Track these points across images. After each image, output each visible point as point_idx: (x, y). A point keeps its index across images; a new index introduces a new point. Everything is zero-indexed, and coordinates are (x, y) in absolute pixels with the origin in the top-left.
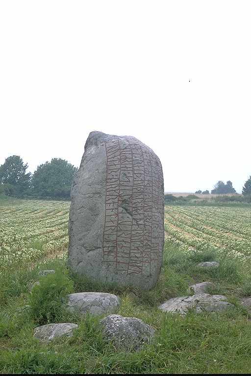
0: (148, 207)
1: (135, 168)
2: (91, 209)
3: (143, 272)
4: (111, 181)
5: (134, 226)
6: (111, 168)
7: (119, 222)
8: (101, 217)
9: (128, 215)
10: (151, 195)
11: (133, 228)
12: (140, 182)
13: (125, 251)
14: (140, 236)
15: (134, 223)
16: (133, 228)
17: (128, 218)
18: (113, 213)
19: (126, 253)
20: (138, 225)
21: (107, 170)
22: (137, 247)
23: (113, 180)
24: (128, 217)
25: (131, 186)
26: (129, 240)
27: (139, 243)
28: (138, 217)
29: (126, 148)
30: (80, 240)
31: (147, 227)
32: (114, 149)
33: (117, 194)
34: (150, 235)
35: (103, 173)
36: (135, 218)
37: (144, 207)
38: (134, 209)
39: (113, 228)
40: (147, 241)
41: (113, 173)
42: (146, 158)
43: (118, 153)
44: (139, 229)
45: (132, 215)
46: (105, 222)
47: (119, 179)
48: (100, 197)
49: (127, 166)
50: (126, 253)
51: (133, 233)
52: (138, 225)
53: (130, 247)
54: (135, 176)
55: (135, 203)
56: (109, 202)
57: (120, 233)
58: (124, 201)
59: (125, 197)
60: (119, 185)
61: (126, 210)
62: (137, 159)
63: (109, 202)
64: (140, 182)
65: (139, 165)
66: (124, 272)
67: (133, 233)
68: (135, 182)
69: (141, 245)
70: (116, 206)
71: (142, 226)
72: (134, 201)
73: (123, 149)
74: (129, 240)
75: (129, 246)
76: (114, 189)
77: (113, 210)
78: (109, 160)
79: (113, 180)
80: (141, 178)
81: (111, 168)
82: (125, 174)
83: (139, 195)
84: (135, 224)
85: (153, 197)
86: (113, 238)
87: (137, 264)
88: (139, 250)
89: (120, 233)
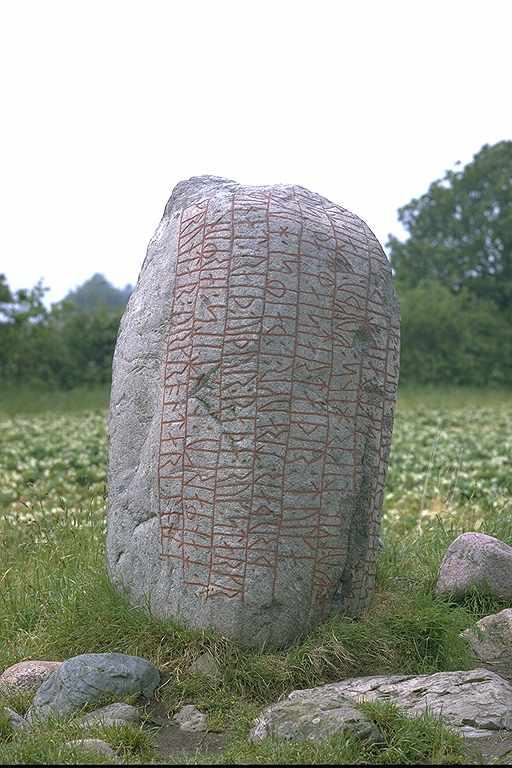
0: (273, 398)
1: (237, 280)
2: (139, 402)
3: (246, 593)
4: (179, 320)
5: (225, 454)
6: (183, 281)
7: (189, 440)
8: (153, 430)
9: (210, 421)
10: (287, 362)
11: (221, 462)
12: (243, 322)
13: (201, 529)
14: (242, 484)
15: (225, 444)
16: (221, 462)
17: (210, 429)
18: (174, 415)
19: (203, 535)
20: (235, 451)
21: (174, 290)
22: (229, 518)
23: (183, 317)
24: (209, 429)
25: (221, 335)
26: (208, 495)
27: (236, 506)
28: (238, 426)
29: (219, 222)
30: (121, 489)
31: (265, 460)
32: (196, 226)
33: (187, 359)
34: (280, 480)
35: (167, 295)
36: (226, 429)
37: (255, 396)
38: (224, 405)
39: (174, 458)
40: (264, 502)
41: (185, 298)
42: (282, 248)
43: (200, 236)
44: (238, 464)
45: (220, 422)
46: (162, 441)
47: (192, 312)
48: (156, 367)
49: (216, 274)
50: (203, 535)
51: (221, 474)
52: (235, 451)
53: (212, 518)
54: (232, 305)
55: (231, 385)
56: (170, 382)
57: (189, 475)
58: (202, 379)
59: (203, 366)
60: (194, 332)
61: (207, 406)
62: (244, 252)
63: (170, 382)
64: (243, 322)
65: (248, 270)
66: (200, 588)
67: (221, 474)
68: (232, 324)
69: (244, 512)
70: (182, 394)
71: (249, 456)
72: (226, 380)
73: (213, 225)
74: (208, 495)
75: (210, 514)
76: (182, 344)
77: (176, 404)
78: (182, 258)
79: (183, 317)
80: (248, 309)
81: (183, 281)
82: (206, 300)
83: (247, 361)
84: (229, 448)
85: (295, 367)
86: (175, 487)
87: (229, 569)
88: (237, 527)
89: (189, 475)
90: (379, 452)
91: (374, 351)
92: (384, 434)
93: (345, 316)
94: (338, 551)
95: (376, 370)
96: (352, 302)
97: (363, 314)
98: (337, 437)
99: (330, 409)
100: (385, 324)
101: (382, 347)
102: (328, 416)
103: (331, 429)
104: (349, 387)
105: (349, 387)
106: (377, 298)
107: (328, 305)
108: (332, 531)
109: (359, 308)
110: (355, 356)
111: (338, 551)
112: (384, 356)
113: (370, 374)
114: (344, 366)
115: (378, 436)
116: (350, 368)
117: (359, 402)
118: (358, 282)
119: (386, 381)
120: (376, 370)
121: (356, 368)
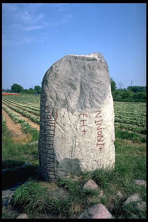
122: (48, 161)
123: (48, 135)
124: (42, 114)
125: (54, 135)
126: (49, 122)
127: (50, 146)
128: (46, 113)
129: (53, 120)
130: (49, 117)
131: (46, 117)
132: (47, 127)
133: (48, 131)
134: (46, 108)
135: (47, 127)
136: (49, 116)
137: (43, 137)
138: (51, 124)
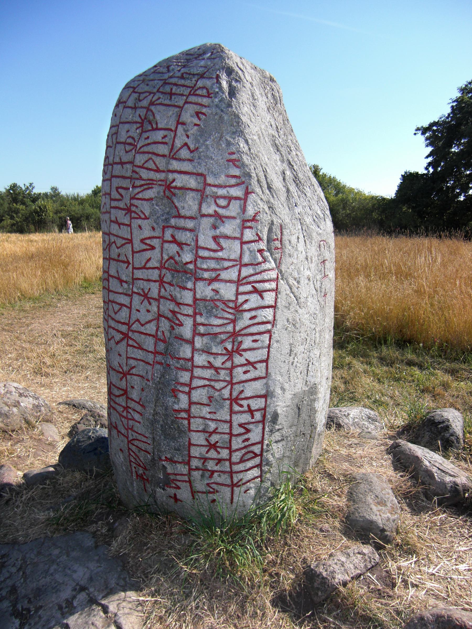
90: (192, 342)
91: (177, 219)
92: (199, 319)
93: (143, 182)
94: (144, 439)
95: (180, 244)
96: (150, 165)
97: (162, 176)
98: (138, 320)
99: (135, 290)
100: (192, 182)
101: (188, 214)
102: (131, 296)
103: (134, 311)
104: (149, 265)
105: (149, 265)
106: (184, 153)
107: (129, 174)
108: (137, 416)
109: (158, 171)
110: (153, 229)
111: (144, 439)
112: (190, 224)
113: (173, 249)
114: (142, 241)
115: (188, 323)
116: (148, 241)
117: (161, 281)
118: (160, 139)
119: (197, 256)
120: (180, 244)
121: (155, 243)
122: (241, 425)
123: (254, 329)
124: (222, 249)
125: (273, 323)
126: (258, 277)
127: (255, 368)
128: (245, 247)
129: (273, 269)
130: (260, 259)
131: (246, 260)
132: (246, 301)
133: (253, 313)
134: (249, 224)
135: (246, 301)
136: (259, 255)
137: (223, 341)
138: (267, 286)
